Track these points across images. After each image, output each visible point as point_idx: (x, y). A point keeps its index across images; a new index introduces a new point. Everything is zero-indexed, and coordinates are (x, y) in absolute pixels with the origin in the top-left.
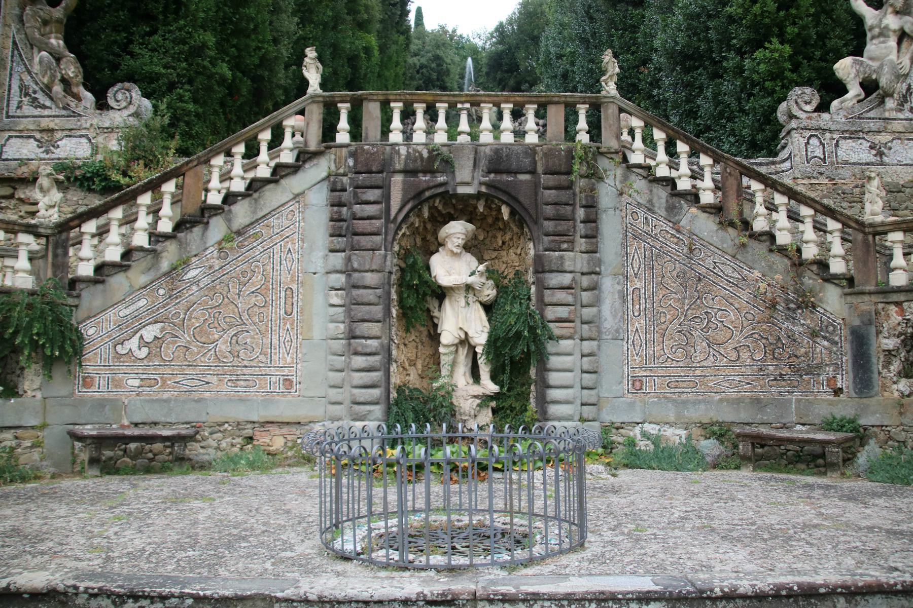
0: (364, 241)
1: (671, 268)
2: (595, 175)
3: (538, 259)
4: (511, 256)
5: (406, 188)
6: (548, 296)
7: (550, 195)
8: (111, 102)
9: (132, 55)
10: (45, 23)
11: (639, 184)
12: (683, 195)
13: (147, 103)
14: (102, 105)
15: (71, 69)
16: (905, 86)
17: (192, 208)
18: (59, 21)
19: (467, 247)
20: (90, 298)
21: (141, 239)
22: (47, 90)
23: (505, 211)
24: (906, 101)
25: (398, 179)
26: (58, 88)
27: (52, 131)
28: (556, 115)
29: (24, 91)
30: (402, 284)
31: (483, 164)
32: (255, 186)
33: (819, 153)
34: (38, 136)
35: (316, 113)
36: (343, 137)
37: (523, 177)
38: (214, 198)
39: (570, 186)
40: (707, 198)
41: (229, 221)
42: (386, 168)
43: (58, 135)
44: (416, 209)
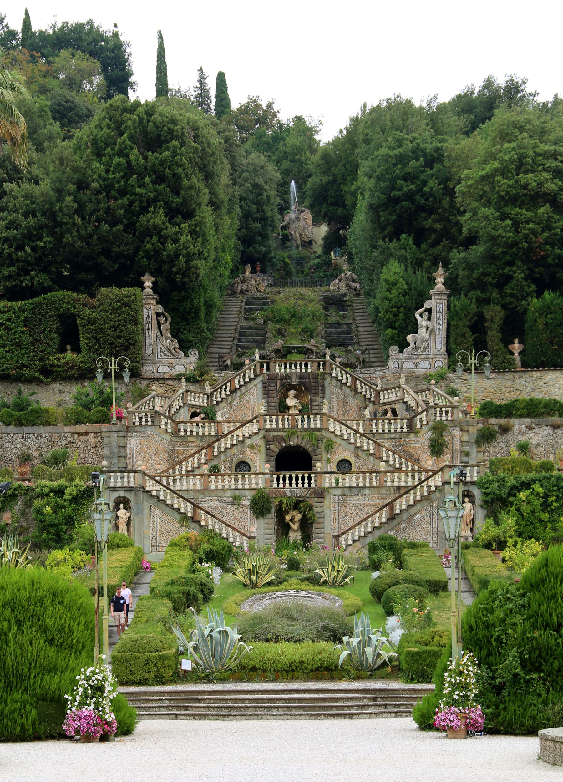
0: (271, 396)
1: (340, 401)
2: (323, 379)
3: (311, 399)
4: (305, 399)
5: (280, 383)
6: (313, 408)
7: (313, 384)
11: (334, 381)
12: (344, 384)
14: (186, 355)
16: (426, 345)
17: (233, 389)
19: (295, 397)
20: (217, 408)
21: (224, 396)
22: (169, 351)
23: (303, 388)
25: (278, 381)
28: (316, 365)
29: (161, 351)
30: (279, 405)
33: (397, 366)
35: (258, 366)
36: (265, 371)
38: (237, 386)
39: (318, 382)
42: (276, 378)
44: (283, 388)
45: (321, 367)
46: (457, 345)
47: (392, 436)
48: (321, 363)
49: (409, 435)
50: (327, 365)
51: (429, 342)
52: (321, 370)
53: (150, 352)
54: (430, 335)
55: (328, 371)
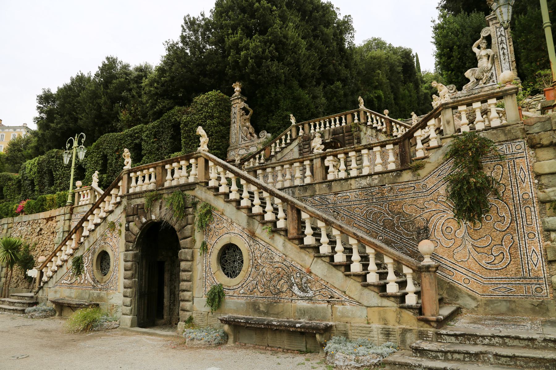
8: (260, 136)
9: (268, 122)
10: (245, 120)
13: (269, 135)
15: (251, 130)
16: (490, 74)
17: (267, 156)
18: (248, 119)
22: (246, 136)
24: (491, 79)
26: (249, 135)
27: (248, 146)
28: (349, 117)
31: (331, 134)
32: (282, 149)
34: (245, 148)
35: (294, 130)
36: (300, 134)
37: (340, 135)
38: (273, 153)
39: (352, 134)
40: (384, 130)
41: (276, 158)
43: (249, 147)
45: (356, 118)
46: (532, 63)
47: (364, 182)
48: (356, 114)
49: (399, 176)
50: (362, 113)
51: (493, 71)
52: (356, 121)
53: (234, 140)
54: (493, 63)
55: (362, 121)
